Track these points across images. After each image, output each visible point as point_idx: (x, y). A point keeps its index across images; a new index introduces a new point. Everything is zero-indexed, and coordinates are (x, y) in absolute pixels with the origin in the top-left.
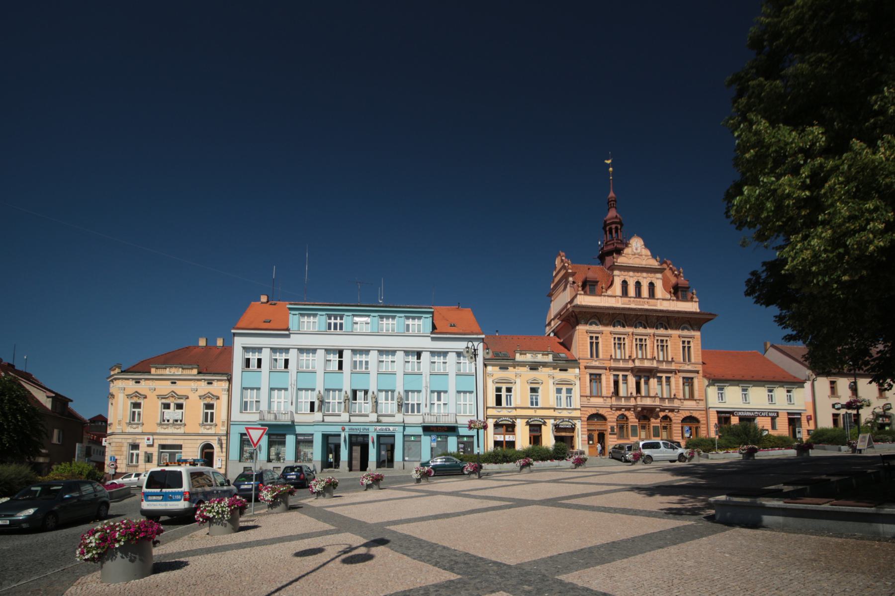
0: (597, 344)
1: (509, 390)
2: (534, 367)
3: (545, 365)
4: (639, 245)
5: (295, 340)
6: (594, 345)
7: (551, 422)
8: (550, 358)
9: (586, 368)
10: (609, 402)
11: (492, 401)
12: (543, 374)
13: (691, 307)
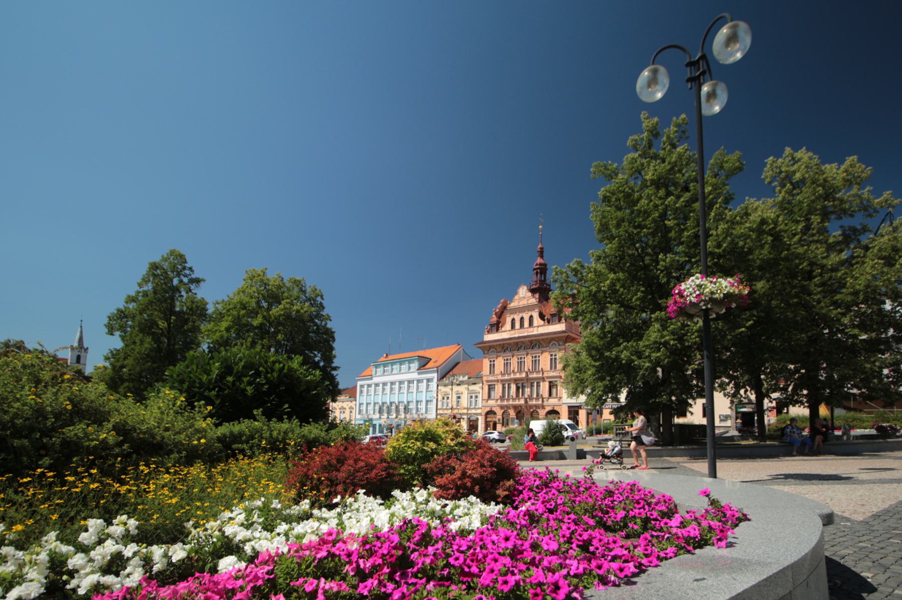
0: (494, 365)
1: (448, 398)
4: (524, 290)
5: (376, 380)
6: (492, 367)
7: (465, 417)
8: (466, 378)
10: (499, 402)
12: (462, 388)
13: (560, 327)
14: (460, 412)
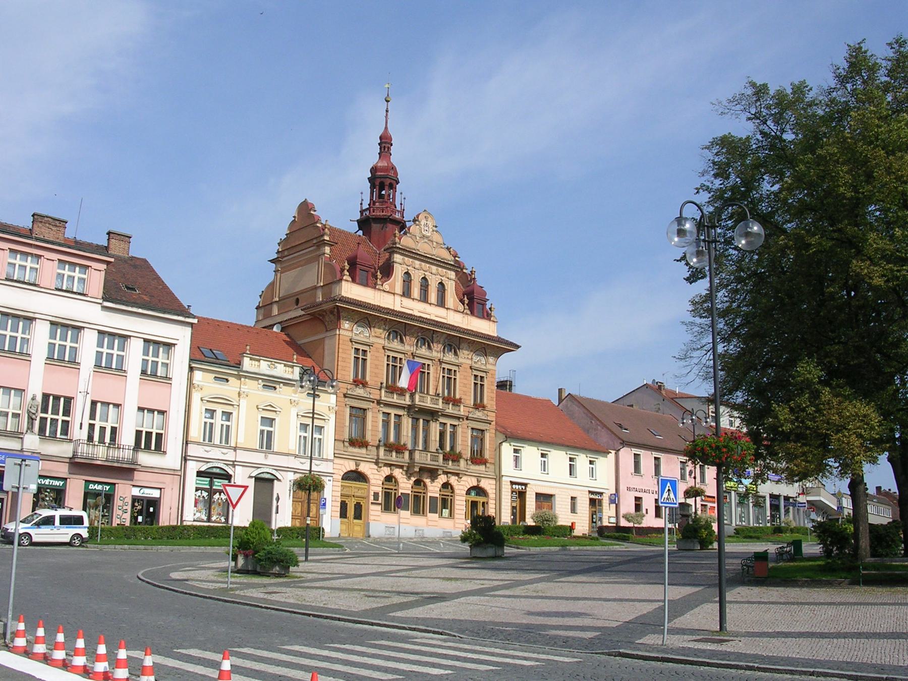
2: (271, 383)
3: (287, 382)
9: (345, 396)
11: (196, 432)
14: (273, 460)
